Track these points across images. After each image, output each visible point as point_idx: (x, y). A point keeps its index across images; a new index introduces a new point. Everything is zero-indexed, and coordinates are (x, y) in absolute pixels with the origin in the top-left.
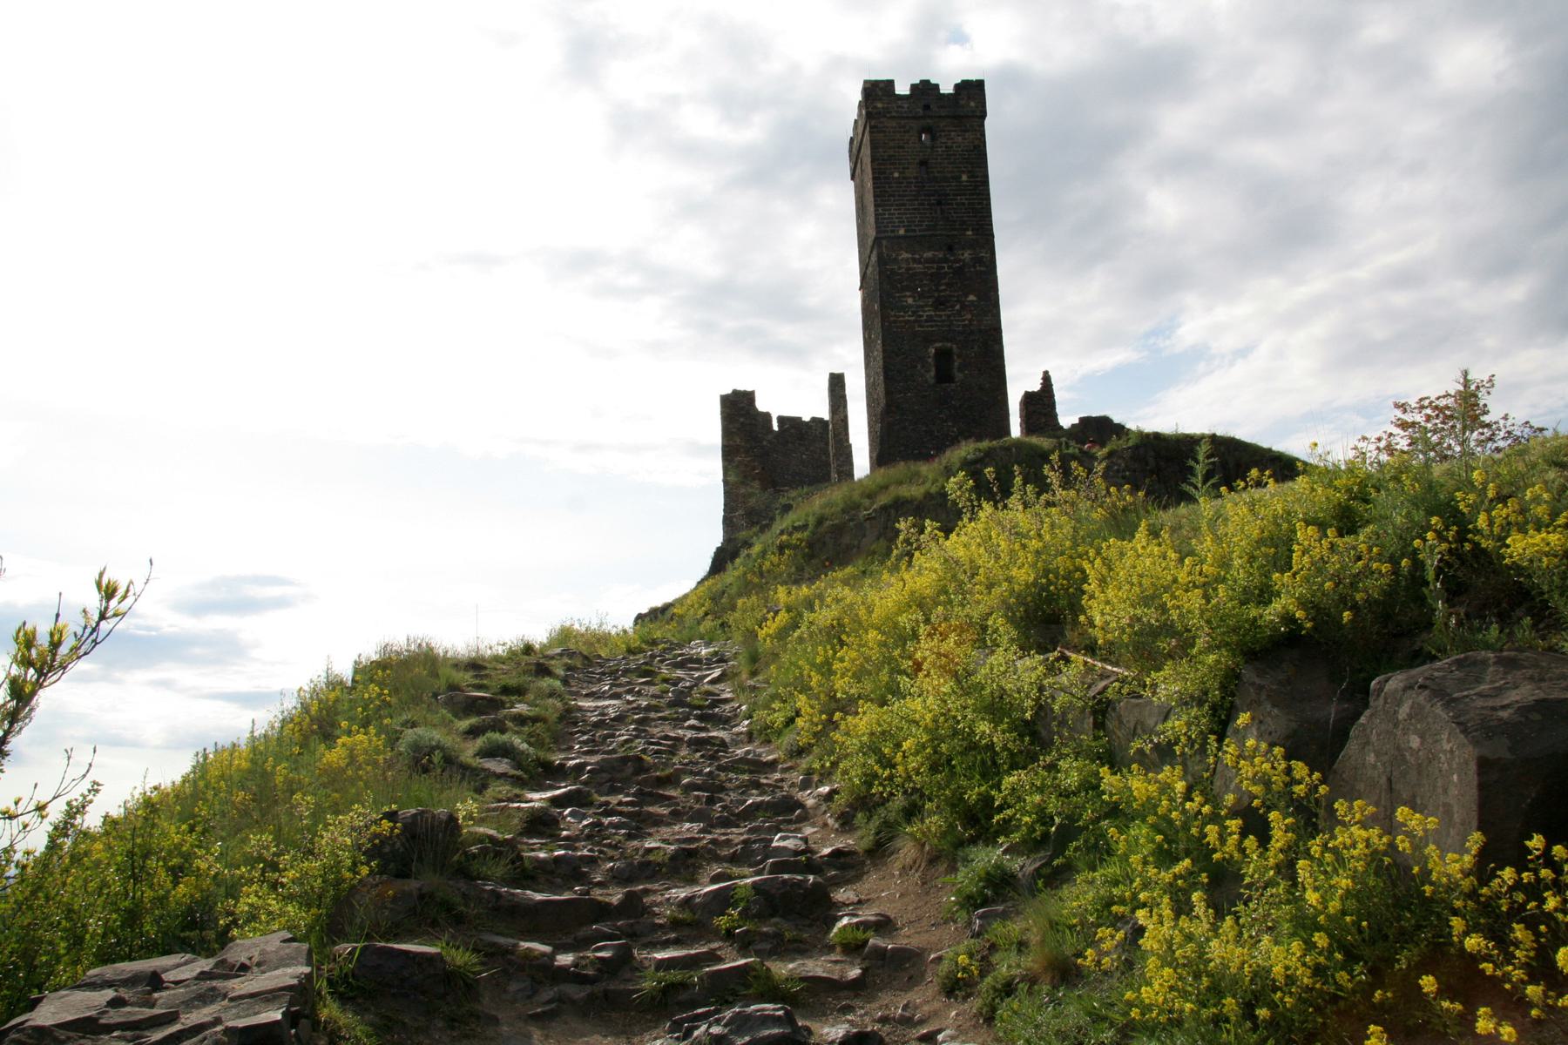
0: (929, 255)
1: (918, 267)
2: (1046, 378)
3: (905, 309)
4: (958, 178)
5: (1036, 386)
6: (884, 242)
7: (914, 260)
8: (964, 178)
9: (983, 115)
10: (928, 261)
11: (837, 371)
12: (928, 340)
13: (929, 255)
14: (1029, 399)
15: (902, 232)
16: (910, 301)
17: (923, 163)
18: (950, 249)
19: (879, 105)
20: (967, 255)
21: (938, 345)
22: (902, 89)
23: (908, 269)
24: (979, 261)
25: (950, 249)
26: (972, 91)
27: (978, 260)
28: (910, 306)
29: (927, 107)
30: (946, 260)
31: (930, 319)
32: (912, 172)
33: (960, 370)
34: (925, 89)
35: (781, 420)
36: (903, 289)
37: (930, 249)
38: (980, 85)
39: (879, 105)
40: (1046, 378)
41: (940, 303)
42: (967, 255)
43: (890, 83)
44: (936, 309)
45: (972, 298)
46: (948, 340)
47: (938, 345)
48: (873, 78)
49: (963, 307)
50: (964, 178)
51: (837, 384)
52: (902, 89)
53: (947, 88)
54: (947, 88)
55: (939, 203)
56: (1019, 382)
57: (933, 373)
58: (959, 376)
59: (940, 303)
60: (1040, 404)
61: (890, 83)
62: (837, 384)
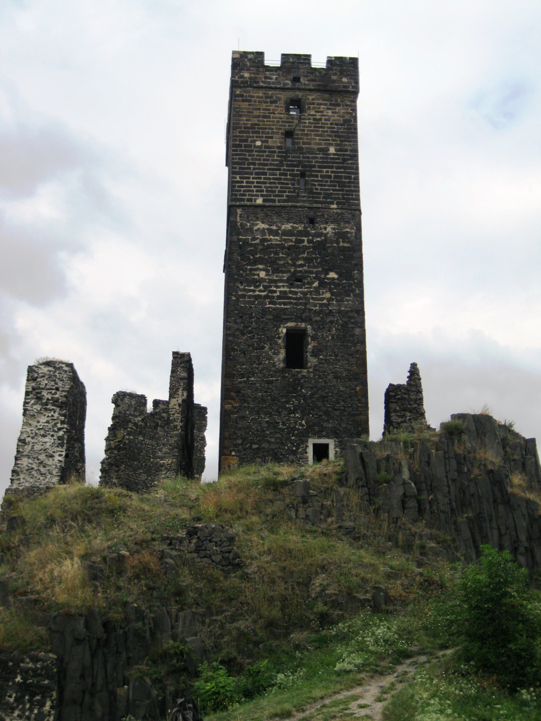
0: (288, 226)
1: (275, 239)
2: (414, 371)
3: (257, 282)
4: (325, 151)
5: (402, 379)
6: (239, 211)
7: (271, 232)
8: (332, 150)
9: (356, 93)
10: (286, 233)
11: (182, 351)
12: (279, 317)
13: (288, 226)
14: (393, 394)
15: (260, 201)
16: (262, 274)
17: (289, 134)
18: (312, 221)
19: (246, 75)
20: (329, 229)
21: (290, 324)
22: (273, 60)
23: (263, 241)
24: (341, 235)
25: (312, 221)
26: (345, 69)
27: (341, 235)
28: (262, 280)
29: (296, 80)
30: (307, 234)
31: (283, 296)
32: (276, 141)
33: (315, 354)
34: (295, 63)
35: (156, 403)
36: (256, 262)
37: (288, 221)
38: (354, 62)
39: (246, 75)
40: (414, 371)
41: (296, 279)
42: (329, 229)
43: (261, 55)
44: (291, 285)
45: (332, 275)
46: (303, 321)
47: (290, 324)
48: (242, 49)
49: (322, 284)
50: (332, 150)
51: (182, 365)
52: (273, 60)
53: (319, 62)
54: (319, 62)
55: (303, 175)
56: (382, 374)
57: (282, 354)
58: (312, 361)
59: (296, 279)
60: (405, 399)
61: (261, 55)
62: (182, 365)
